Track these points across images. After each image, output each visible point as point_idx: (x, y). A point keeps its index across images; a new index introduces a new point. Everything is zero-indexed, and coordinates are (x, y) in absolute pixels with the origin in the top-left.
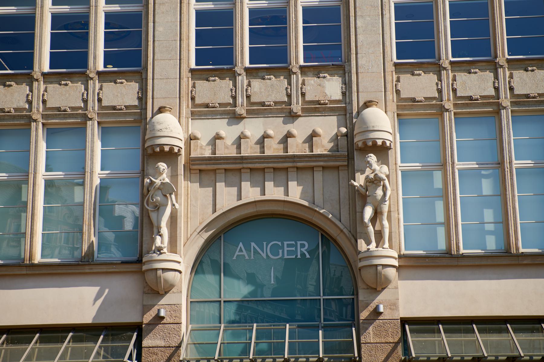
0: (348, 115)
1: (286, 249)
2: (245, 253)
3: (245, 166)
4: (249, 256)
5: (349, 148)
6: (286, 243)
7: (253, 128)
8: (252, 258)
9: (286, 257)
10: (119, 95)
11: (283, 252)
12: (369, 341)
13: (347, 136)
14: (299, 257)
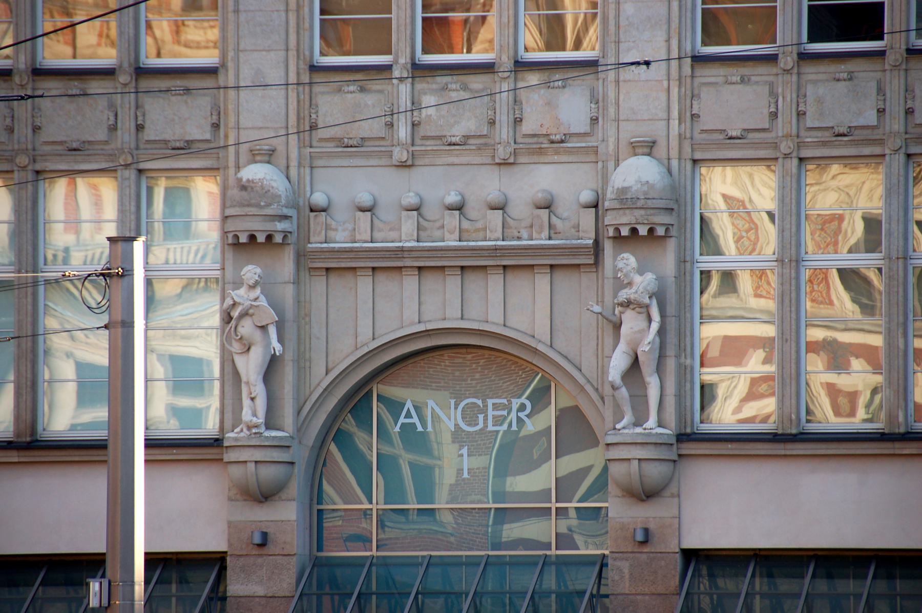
1: (491, 413)
2: (415, 420)
3: (408, 263)
6: (490, 402)
9: (490, 428)
11: (486, 419)
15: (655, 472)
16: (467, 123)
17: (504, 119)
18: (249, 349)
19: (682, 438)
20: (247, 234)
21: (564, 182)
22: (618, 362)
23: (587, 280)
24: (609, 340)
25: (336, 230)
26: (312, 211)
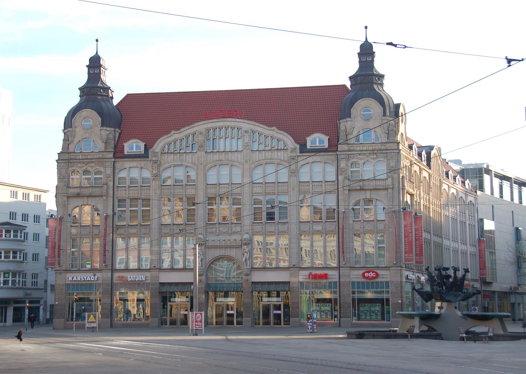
7: (222, 238)
15: (248, 272)
16: (225, 230)
17: (230, 230)
19: (252, 268)
21: (237, 237)
22: (244, 259)
23: (240, 249)
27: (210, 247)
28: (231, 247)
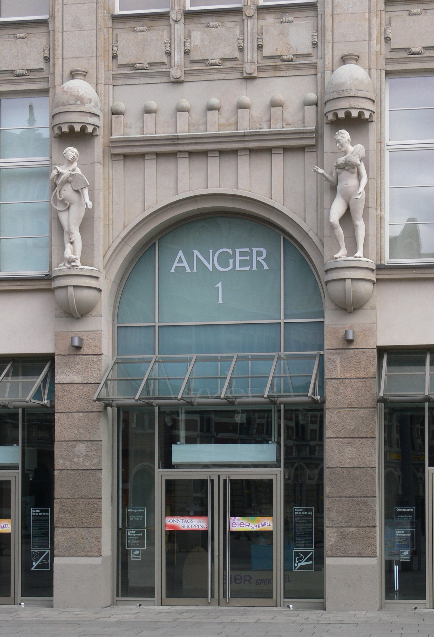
0: (319, 75)
1: (238, 258)
2: (185, 264)
3: (182, 148)
4: (191, 268)
5: (319, 122)
6: (238, 251)
8: (195, 270)
9: (238, 268)
10: (20, 55)
12: (336, 377)
13: (316, 105)
14: (255, 268)
18: (69, 208)
20: (67, 125)
23: (310, 157)
24: (327, 197)
25: (131, 127)
26: (113, 114)
27: (130, 153)
28: (258, 147)
